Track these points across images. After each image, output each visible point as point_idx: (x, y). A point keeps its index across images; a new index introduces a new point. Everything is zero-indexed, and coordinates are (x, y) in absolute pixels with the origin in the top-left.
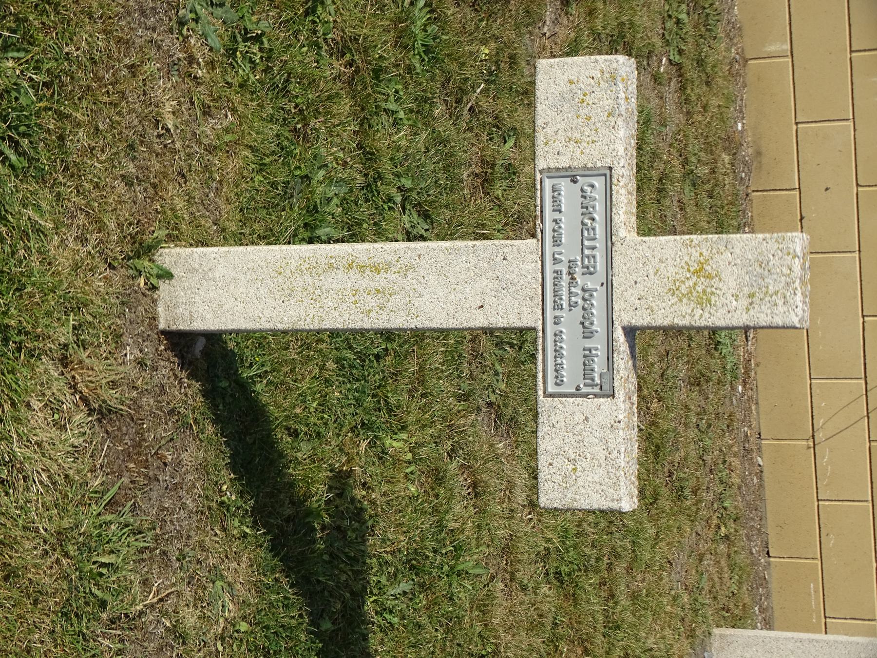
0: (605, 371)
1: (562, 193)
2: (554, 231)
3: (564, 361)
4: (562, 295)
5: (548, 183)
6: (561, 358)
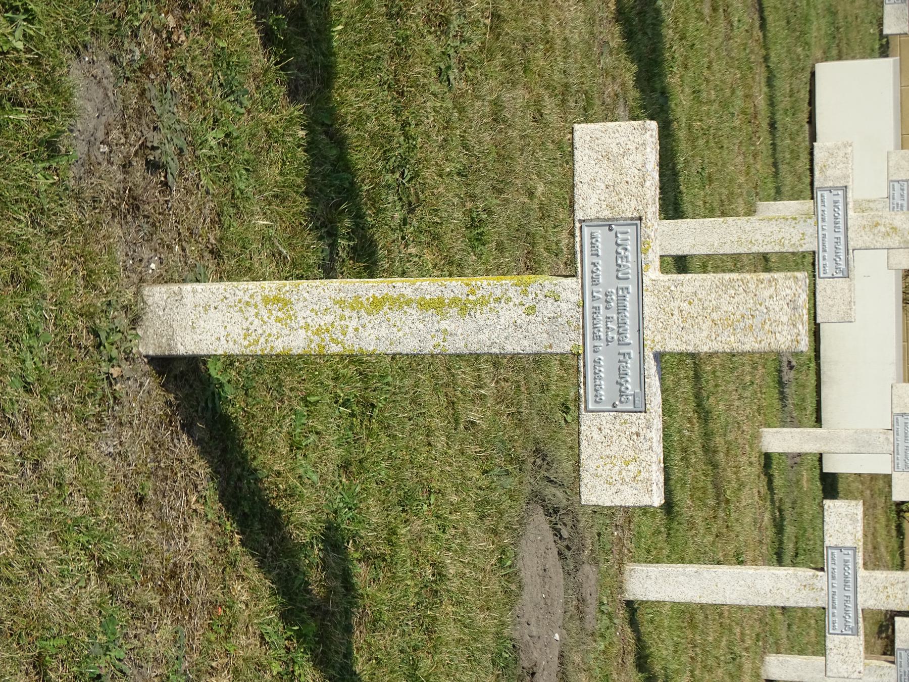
0: (638, 390)
1: (599, 240)
2: (593, 272)
3: (603, 382)
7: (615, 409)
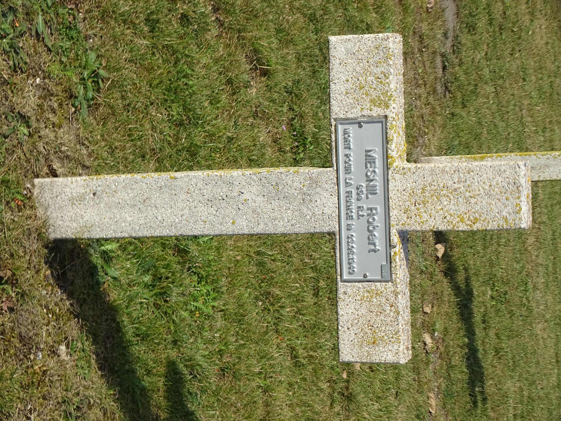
0: (385, 263)
1: (351, 135)
2: (346, 162)
3: (355, 257)
4: (352, 209)
5: (340, 128)
6: (353, 254)
7: (365, 279)
